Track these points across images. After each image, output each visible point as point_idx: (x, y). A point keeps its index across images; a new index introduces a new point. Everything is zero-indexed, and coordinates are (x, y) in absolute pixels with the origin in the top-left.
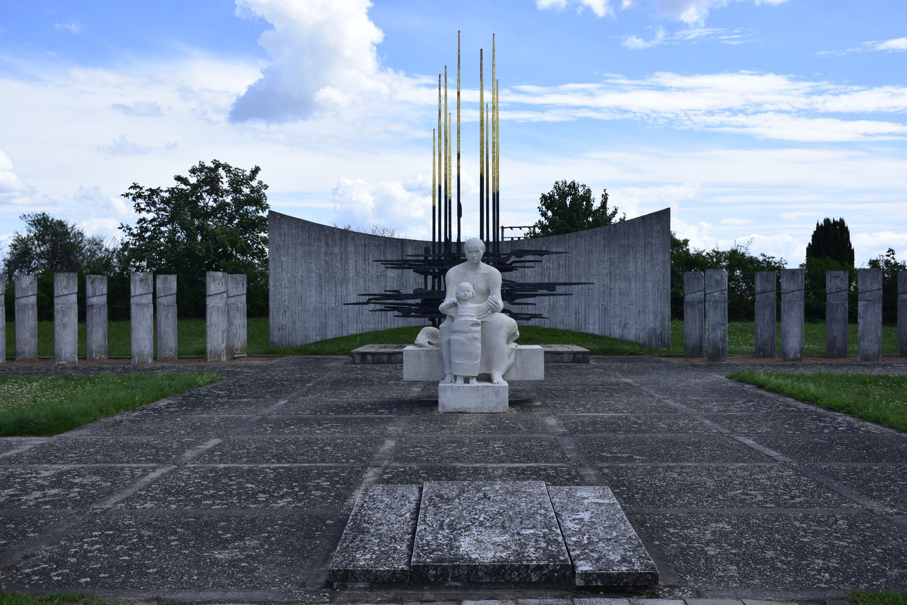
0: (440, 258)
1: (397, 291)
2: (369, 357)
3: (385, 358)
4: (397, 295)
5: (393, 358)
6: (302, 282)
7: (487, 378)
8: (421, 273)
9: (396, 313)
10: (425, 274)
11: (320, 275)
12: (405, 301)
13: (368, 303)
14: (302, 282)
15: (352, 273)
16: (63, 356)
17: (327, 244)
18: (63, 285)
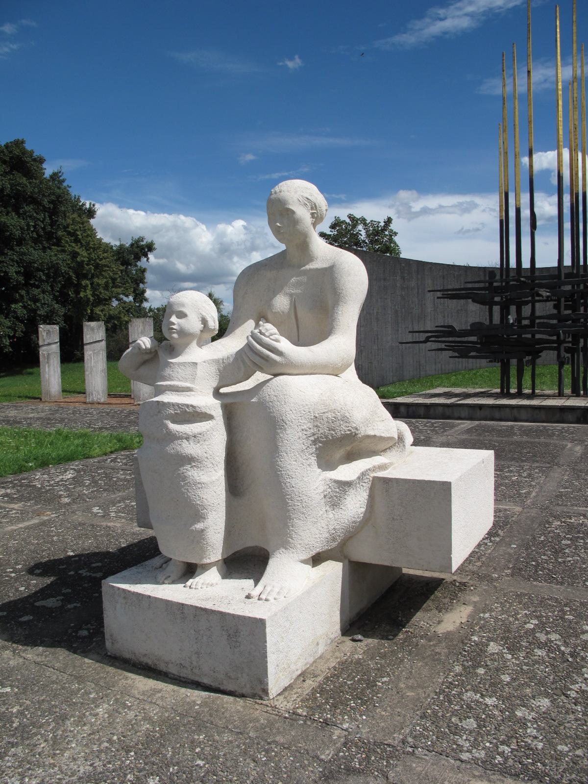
0: (507, 283)
1: (451, 327)
2: (402, 409)
3: (422, 411)
4: (450, 331)
5: (432, 411)
6: (378, 320)
7: (246, 562)
8: (482, 303)
9: (450, 353)
10: (491, 304)
11: (396, 312)
12: (465, 339)
13: (425, 341)
14: (378, 320)
15: (429, 309)
16: (142, 396)
17: (403, 278)
18: (140, 331)
